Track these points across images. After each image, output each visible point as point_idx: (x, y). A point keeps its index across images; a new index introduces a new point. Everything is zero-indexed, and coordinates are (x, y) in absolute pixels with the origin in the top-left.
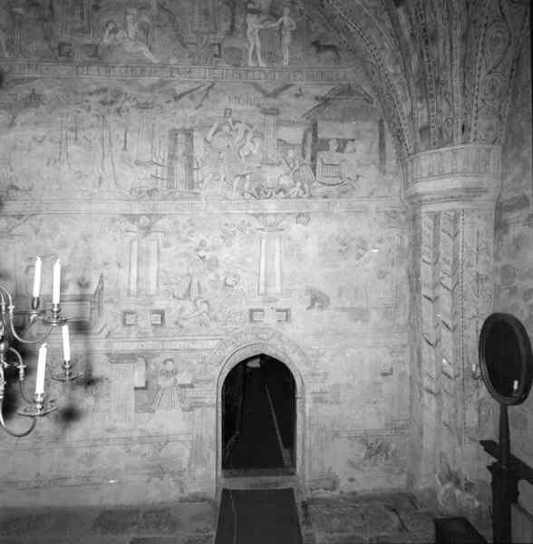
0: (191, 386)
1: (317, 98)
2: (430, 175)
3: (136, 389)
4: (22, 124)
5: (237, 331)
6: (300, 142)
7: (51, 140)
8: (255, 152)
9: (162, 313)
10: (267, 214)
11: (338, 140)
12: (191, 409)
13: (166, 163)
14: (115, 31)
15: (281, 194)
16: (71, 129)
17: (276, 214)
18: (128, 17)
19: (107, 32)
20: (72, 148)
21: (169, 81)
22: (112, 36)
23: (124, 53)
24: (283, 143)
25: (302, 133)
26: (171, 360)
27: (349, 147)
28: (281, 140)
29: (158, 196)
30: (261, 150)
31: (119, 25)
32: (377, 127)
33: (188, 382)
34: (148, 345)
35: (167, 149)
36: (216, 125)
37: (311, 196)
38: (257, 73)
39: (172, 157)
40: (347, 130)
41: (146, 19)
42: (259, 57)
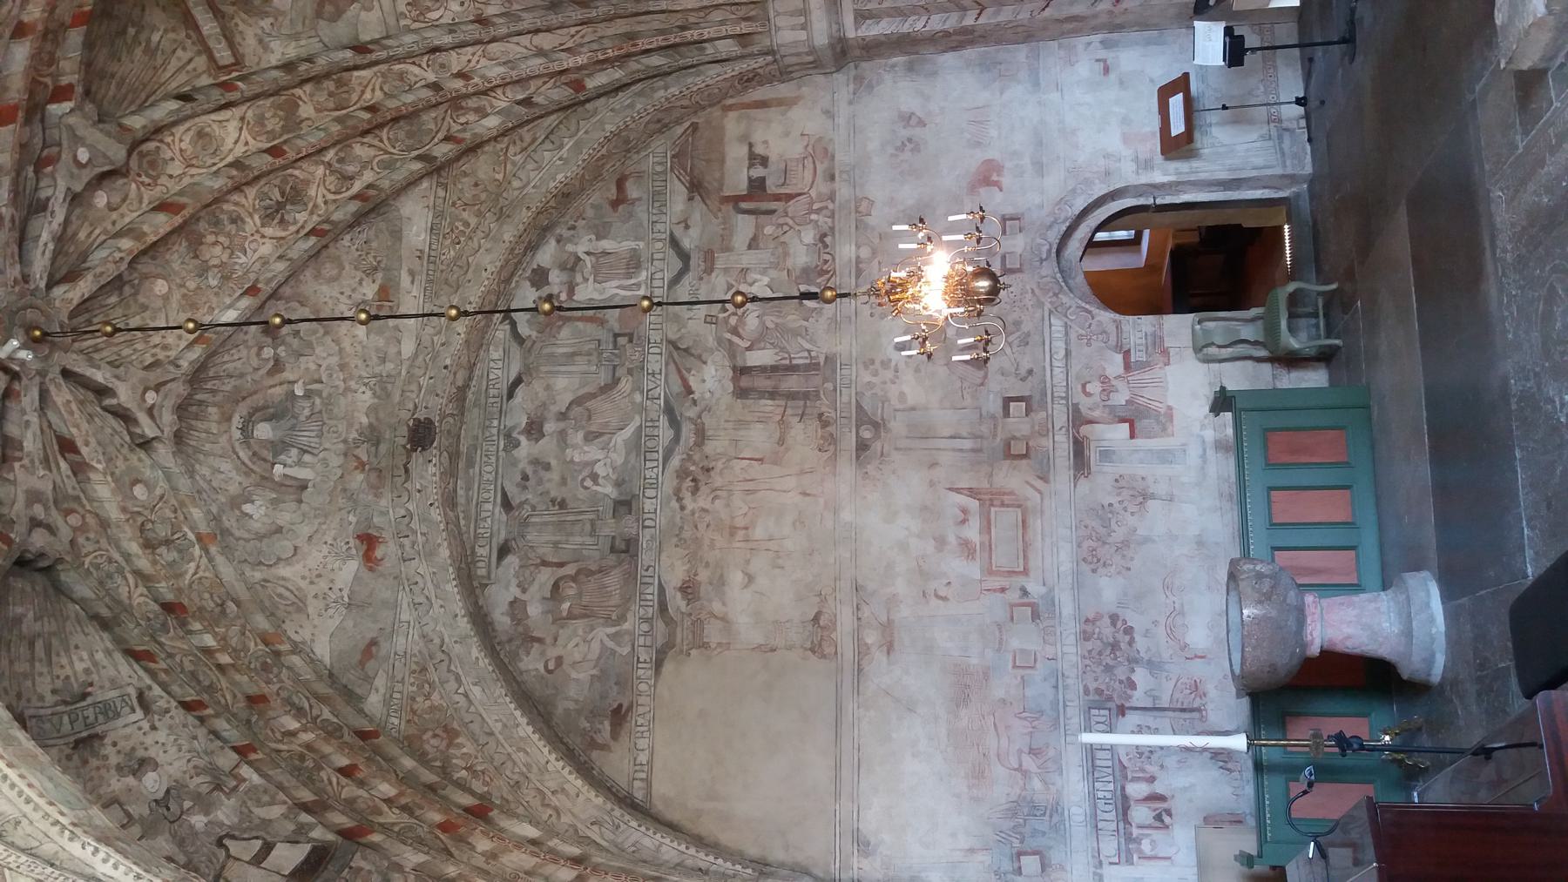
0: (1127, 354)
1: (691, 199)
2: (804, 27)
3: (1132, 436)
4: (724, 604)
5: (1037, 291)
6: (753, 217)
7: (748, 562)
8: (766, 280)
9: (1007, 401)
10: (858, 257)
11: (751, 166)
12: (1165, 352)
13: (783, 403)
14: (594, 477)
15: (828, 240)
16: (732, 535)
17: (858, 247)
18: (577, 459)
19: (598, 488)
20: (759, 533)
21: (666, 402)
22: (601, 481)
23: (626, 462)
24: (753, 244)
25: (740, 216)
26: (1084, 386)
27: (759, 150)
28: (750, 247)
29: (830, 414)
30: (764, 272)
31: (585, 473)
32: (732, 115)
33: (1119, 358)
34: (1061, 417)
35: (763, 402)
36: (728, 336)
37: (832, 198)
38: (657, 283)
39: (773, 395)
40: (736, 153)
41: (580, 435)
42: (633, 281)
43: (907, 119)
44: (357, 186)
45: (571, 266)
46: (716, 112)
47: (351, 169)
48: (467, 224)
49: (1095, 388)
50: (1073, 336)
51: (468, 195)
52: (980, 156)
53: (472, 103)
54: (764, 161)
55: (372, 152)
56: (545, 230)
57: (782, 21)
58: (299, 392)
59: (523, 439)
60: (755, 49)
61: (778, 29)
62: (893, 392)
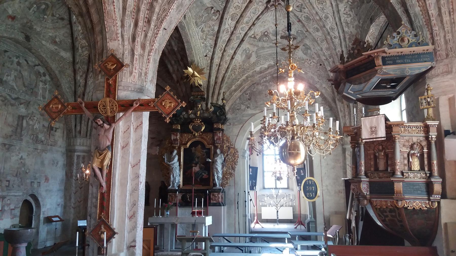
2: (80, 145)
9: (9, 181)
14: (8, 76)
23: (10, 85)
24: (43, 126)
27: (57, 130)
30: (39, 127)
39: (18, 125)
41: (16, 75)
43: (57, 163)
44: (80, 48)
45: (45, 83)
46: (64, 122)
47: (84, 49)
48: (60, 64)
49: (9, 202)
50: (18, 197)
51: (65, 66)
52: (50, 178)
53: (84, 76)
54: (56, 131)
55: (84, 54)
56: (52, 79)
57: (82, 140)
58: (45, 17)
59: (17, 60)
60: (77, 134)
61: (81, 139)
62: (14, 154)
